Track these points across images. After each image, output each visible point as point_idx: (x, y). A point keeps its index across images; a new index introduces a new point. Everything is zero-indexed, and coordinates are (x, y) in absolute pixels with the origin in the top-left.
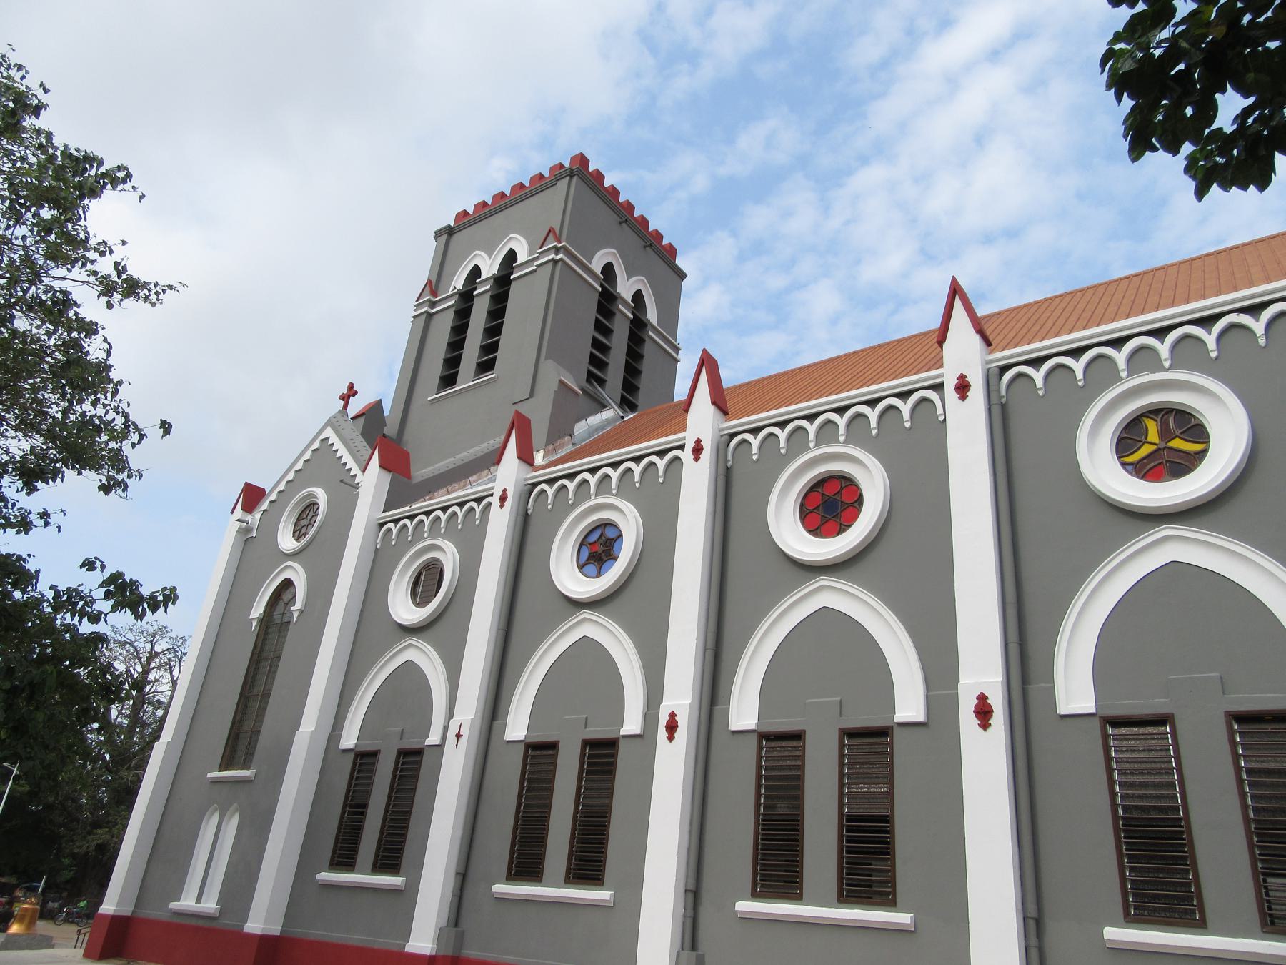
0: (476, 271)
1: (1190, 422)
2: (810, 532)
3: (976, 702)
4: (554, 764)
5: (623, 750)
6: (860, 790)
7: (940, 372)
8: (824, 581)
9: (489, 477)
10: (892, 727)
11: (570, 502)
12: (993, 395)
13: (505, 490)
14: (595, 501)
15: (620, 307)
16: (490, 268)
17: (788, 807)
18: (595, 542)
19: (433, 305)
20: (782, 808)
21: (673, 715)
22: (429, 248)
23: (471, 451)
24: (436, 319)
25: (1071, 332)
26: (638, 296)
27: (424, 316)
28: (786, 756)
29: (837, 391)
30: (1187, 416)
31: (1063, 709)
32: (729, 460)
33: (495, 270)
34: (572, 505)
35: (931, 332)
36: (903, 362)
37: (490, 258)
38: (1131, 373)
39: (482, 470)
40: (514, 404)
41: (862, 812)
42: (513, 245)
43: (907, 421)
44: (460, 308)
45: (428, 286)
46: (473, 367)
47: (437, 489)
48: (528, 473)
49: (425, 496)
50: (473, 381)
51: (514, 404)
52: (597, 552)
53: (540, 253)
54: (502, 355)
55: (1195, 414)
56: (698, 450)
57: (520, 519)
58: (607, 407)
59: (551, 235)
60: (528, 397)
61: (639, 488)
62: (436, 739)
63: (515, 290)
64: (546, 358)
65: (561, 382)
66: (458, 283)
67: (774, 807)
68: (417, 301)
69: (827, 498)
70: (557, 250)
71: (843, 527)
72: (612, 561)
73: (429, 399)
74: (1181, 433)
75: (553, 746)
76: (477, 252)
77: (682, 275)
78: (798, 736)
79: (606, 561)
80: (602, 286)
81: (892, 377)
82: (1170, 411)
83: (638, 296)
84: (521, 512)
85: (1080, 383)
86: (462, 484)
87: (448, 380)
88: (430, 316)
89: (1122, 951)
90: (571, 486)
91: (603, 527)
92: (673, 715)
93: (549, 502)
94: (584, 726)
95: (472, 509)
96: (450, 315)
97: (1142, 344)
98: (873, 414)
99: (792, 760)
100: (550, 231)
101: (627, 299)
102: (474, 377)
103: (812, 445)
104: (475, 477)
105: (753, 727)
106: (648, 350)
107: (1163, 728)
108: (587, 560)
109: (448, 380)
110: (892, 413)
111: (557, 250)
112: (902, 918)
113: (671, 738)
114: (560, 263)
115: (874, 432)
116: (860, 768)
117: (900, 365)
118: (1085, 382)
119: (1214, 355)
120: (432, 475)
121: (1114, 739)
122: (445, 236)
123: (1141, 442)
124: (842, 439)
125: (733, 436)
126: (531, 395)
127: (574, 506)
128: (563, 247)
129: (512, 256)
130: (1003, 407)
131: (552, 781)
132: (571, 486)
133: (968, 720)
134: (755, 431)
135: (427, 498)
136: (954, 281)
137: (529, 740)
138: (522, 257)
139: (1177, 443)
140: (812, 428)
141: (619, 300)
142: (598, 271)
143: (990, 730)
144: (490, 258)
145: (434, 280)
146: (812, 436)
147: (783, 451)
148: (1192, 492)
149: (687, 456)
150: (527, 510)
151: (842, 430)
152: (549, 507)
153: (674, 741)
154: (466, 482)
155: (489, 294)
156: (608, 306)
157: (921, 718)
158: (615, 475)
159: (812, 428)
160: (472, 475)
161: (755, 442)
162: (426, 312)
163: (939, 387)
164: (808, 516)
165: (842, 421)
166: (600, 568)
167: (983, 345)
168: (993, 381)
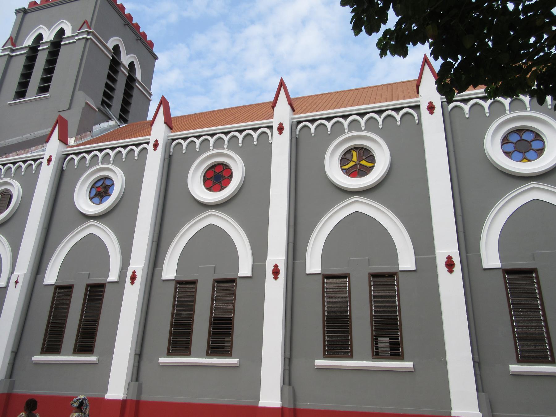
0: (40, 37)
1: (369, 154)
2: (207, 189)
3: (273, 268)
4: (71, 296)
5: (108, 289)
7: (149, 137)
9: (42, 149)
10: (237, 278)
11: (87, 165)
12: (293, 134)
13: (50, 156)
14: (100, 166)
15: (122, 69)
16: (49, 36)
17: (187, 314)
18: (99, 187)
19: (13, 51)
20: (184, 315)
21: (134, 272)
22: (13, 18)
23: (32, 134)
24: (14, 59)
25: (306, 113)
26: (132, 65)
27: (7, 57)
28: (188, 291)
29: (207, 126)
31: (308, 271)
32: (171, 152)
33: (52, 38)
34: (88, 167)
35: (271, 102)
36: (243, 116)
37: (49, 31)
38: (349, 130)
39: (40, 145)
40: (59, 112)
41: (220, 316)
42: (41, 31)
43: (255, 141)
44: (29, 55)
45: (10, 40)
46: (36, 89)
47: (11, 152)
48: (64, 148)
49: (3, 155)
50: (36, 96)
51: (59, 112)
52: (100, 192)
53: (79, 33)
54: (53, 84)
55: (371, 151)
56: (156, 145)
57: (59, 172)
58: (111, 119)
59: (85, 25)
60: (67, 109)
61: (124, 161)
62: (3, 284)
63: (62, 51)
64: (79, 90)
65: (87, 103)
66: (29, 41)
67: (180, 315)
68: (3, 47)
69: (216, 173)
70: (88, 33)
71: (222, 187)
72: (108, 197)
73: (8, 103)
74: (365, 158)
75: (70, 287)
76: (41, 26)
77: (156, 58)
78: (194, 282)
79: (105, 196)
80: (112, 56)
81: (236, 122)
83: (132, 65)
84: (60, 168)
85: (313, 135)
86: (26, 151)
87: (21, 94)
88: (10, 57)
90: (88, 157)
91: (104, 179)
92: (134, 272)
93: (75, 164)
94: (87, 278)
95: (31, 165)
96: (23, 58)
97: (320, 123)
98: (240, 137)
100: (85, 22)
101: (126, 65)
102: (36, 94)
103: (211, 148)
104: (34, 148)
105: (173, 278)
106: (135, 93)
107: (346, 279)
108: (95, 195)
109: (21, 94)
110: (234, 139)
111: (88, 33)
112: (93, 358)
113: (132, 283)
114: (89, 41)
115: (240, 145)
116: (221, 297)
117: (241, 117)
118: (242, 144)
120: (7, 144)
121: (327, 284)
122: (22, 14)
123: (350, 160)
124: (225, 147)
125: (174, 140)
126: (70, 108)
127: (89, 168)
128: (92, 32)
129: (62, 32)
130: (297, 139)
131: (69, 304)
132: (88, 157)
133: (128, 280)
134: (185, 139)
135: (4, 157)
136: (282, 79)
137: (56, 285)
138: (68, 33)
139: (364, 163)
140: (212, 140)
141: (121, 65)
142: (111, 48)
143: (278, 280)
144: (49, 31)
145: (14, 37)
146: (212, 144)
147: (198, 150)
149: (150, 147)
150: (63, 167)
151: (226, 143)
152: (23, 174)
153: (134, 285)
154: (29, 150)
155: (48, 50)
156: (116, 68)
158: (112, 154)
159: (212, 140)
160: (33, 146)
161: (185, 144)
162: (8, 54)
163: (270, 128)
164: (206, 181)
165: (226, 139)
166: (101, 200)
167: (170, 129)
168: (294, 127)
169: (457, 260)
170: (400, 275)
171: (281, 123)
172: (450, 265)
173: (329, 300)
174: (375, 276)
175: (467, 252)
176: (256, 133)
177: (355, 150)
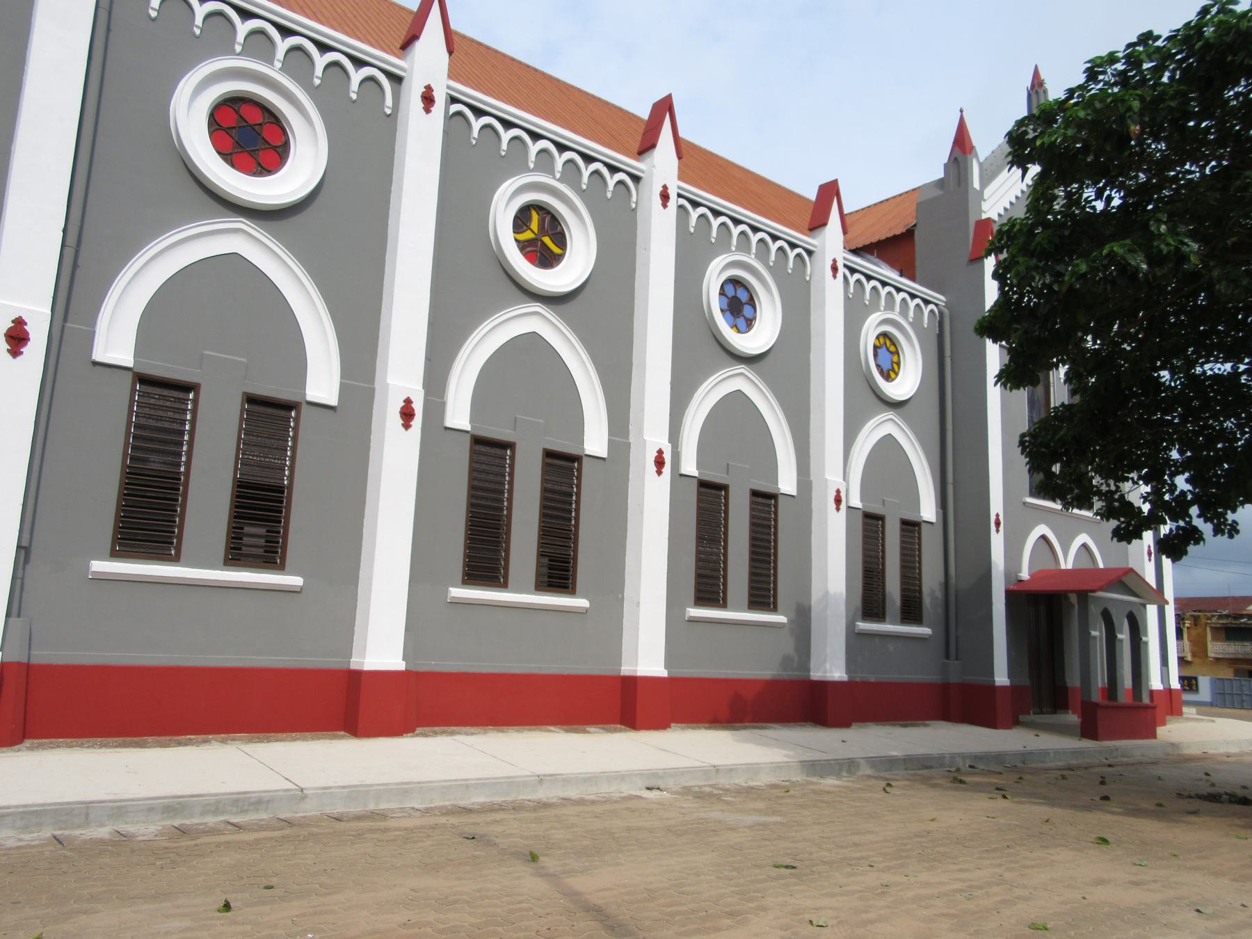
2: (219, 153)
6: (255, 458)
8: (242, 223)
10: (300, 403)
17: (149, 461)
20: (156, 463)
30: (556, 223)
31: (99, 355)
41: (251, 479)
55: (562, 224)
67: (145, 460)
71: (229, 157)
74: (552, 234)
82: (548, 213)
89: (694, 621)
99: (174, 412)
103: (238, 48)
107: (504, 451)
116: (258, 436)
119: (503, 153)
121: (139, 395)
123: (527, 226)
139: (547, 240)
143: (410, 430)
146: (240, 37)
147: (198, 32)
148: (280, 196)
157: (333, 401)
163: (396, 79)
164: (218, 131)
165: (283, 45)
169: (418, 407)
170: (305, 410)
171: (429, 85)
172: (407, 414)
173: (138, 432)
174: (251, 400)
175: (65, 319)
176: (359, 72)
177: (537, 209)
